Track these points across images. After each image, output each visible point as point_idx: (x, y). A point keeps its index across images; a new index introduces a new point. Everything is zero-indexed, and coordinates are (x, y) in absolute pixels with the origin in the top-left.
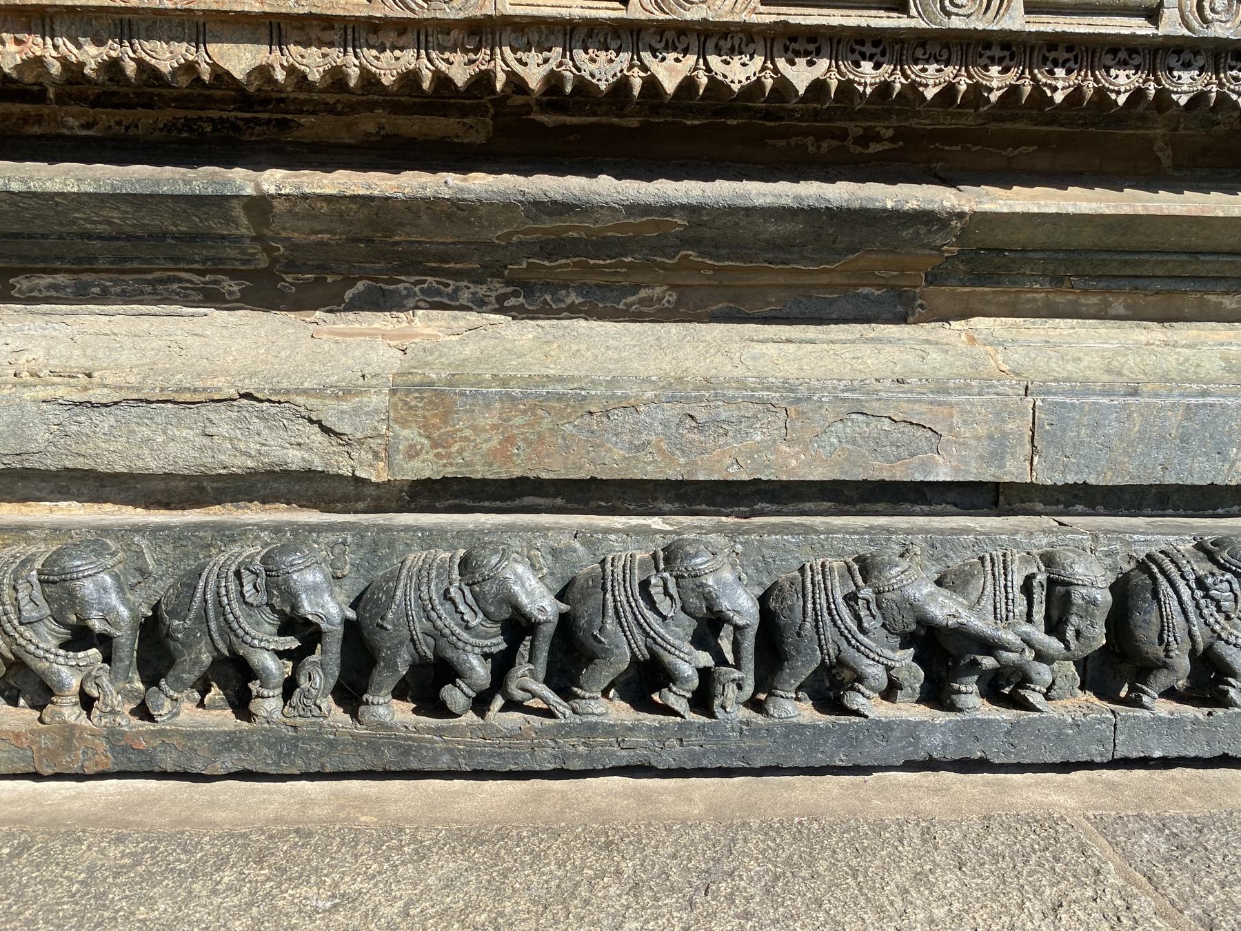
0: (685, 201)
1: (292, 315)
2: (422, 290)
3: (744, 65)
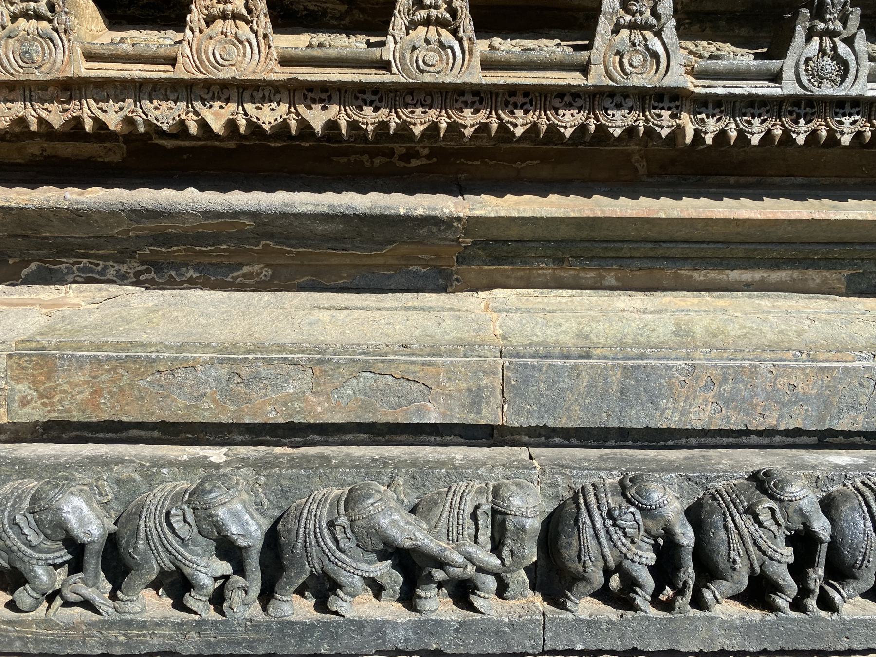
0: (245, 208)
2: (78, 269)
3: (273, 110)
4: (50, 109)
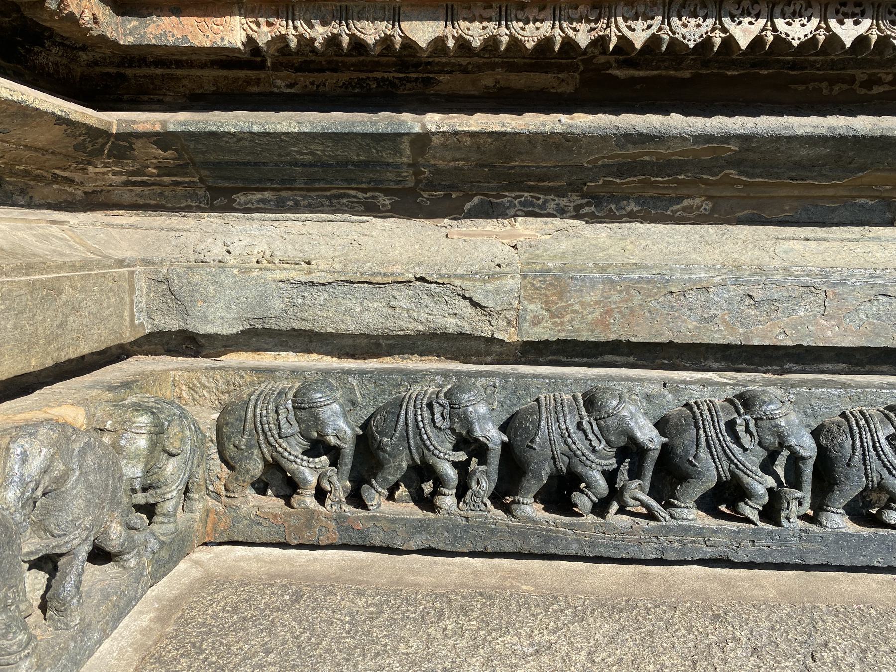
0: (741, 132)
1: (427, 221)
2: (520, 202)
3: (803, 25)
4: (578, 28)
